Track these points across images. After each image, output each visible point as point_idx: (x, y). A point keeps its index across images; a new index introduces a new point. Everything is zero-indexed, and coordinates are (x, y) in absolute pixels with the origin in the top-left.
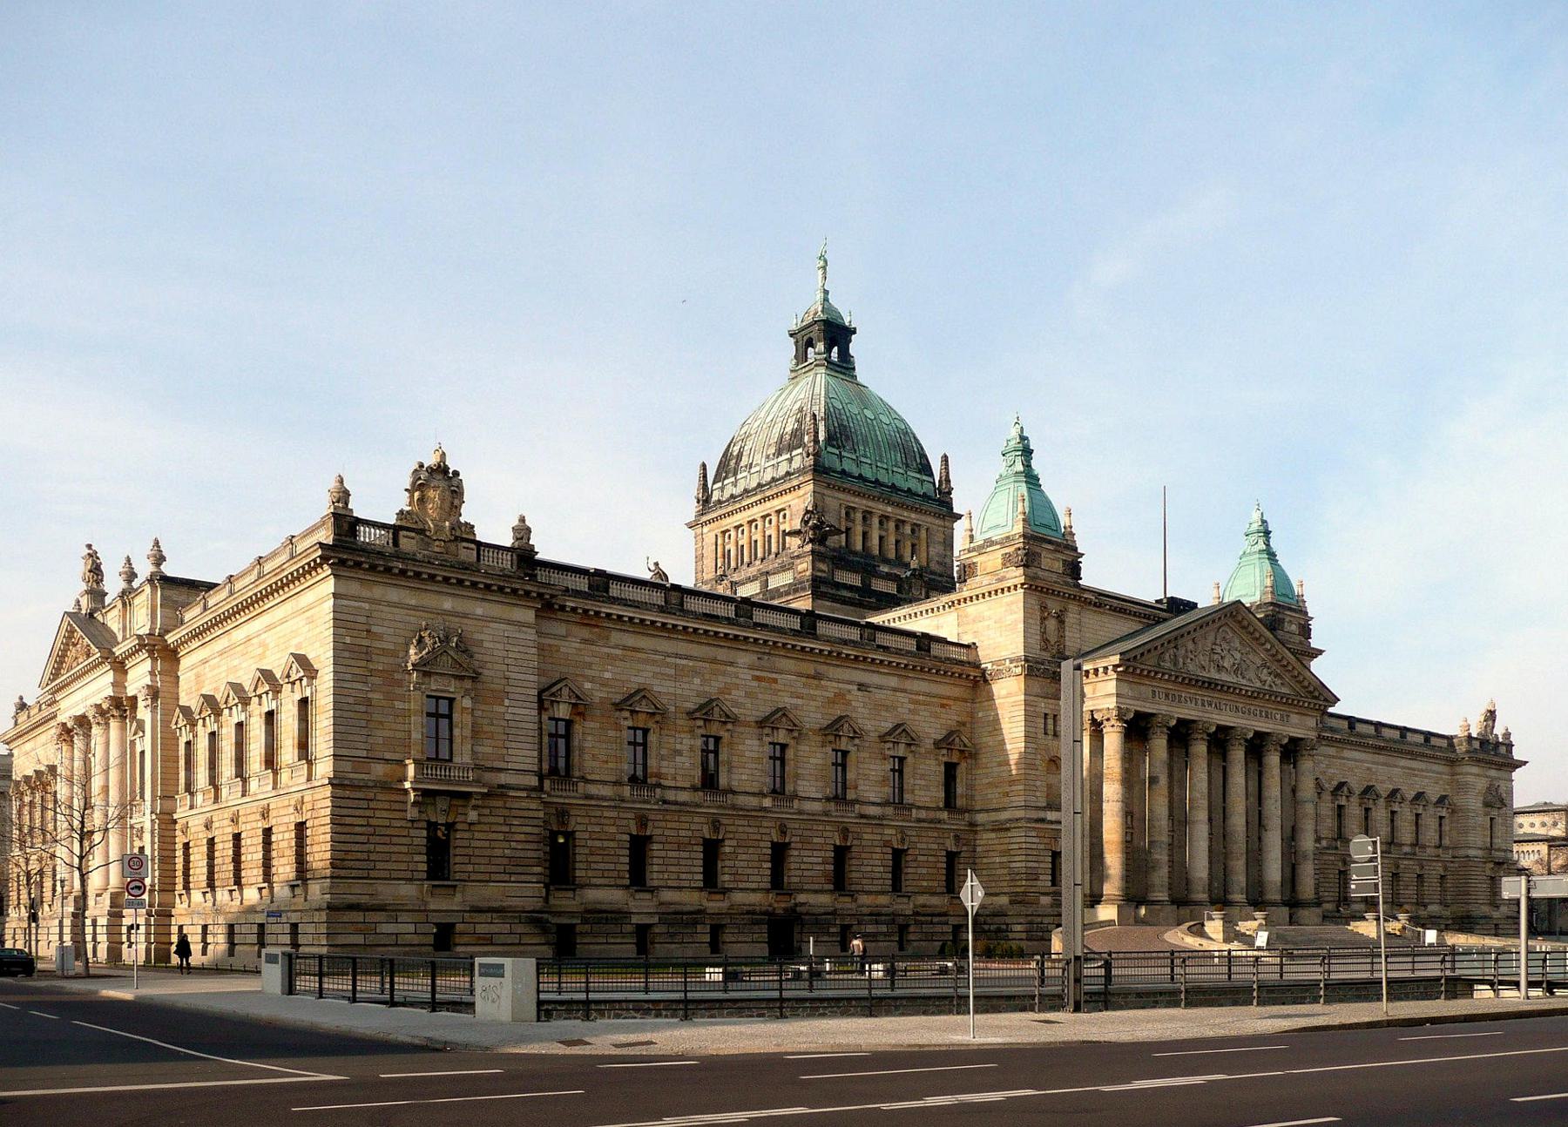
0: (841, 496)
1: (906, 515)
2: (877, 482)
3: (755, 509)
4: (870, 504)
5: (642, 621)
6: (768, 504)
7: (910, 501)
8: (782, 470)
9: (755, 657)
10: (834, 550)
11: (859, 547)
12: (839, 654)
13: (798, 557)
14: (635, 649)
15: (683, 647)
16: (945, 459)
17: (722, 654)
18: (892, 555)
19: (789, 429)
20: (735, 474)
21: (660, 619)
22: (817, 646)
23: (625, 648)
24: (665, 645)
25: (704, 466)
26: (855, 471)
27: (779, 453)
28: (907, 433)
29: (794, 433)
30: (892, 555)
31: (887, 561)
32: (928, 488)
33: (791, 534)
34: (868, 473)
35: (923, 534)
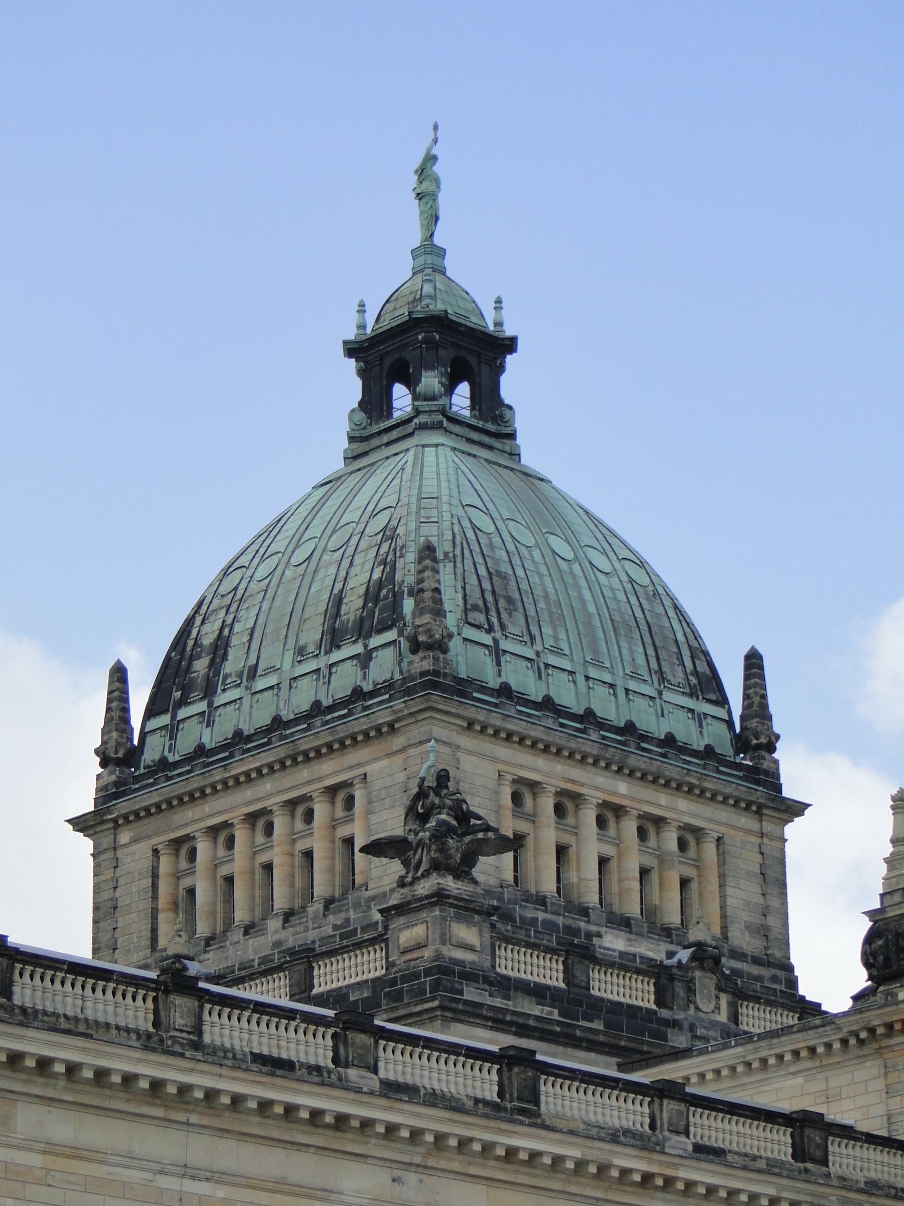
0: (502, 751)
1: (660, 802)
2: (588, 717)
3: (268, 785)
4: (576, 773)
5: (101, 1075)
6: (304, 773)
7: (672, 769)
8: (346, 679)
9: (384, 1177)
10: (488, 893)
11: (549, 886)
12: (603, 1169)
13: (402, 909)
14: (77, 1153)
15: (203, 1149)
16: (754, 663)
17: (301, 1167)
18: (633, 908)
19: (359, 580)
20: (209, 691)
21: (149, 1067)
22: (547, 1145)
23: (51, 1149)
24: (160, 1142)
25: (119, 674)
26: (535, 690)
27: (334, 638)
28: (658, 593)
29: (372, 595)
30: (633, 908)
31: (623, 923)
32: (716, 736)
33: (375, 848)
34: (566, 695)
35: (710, 850)
